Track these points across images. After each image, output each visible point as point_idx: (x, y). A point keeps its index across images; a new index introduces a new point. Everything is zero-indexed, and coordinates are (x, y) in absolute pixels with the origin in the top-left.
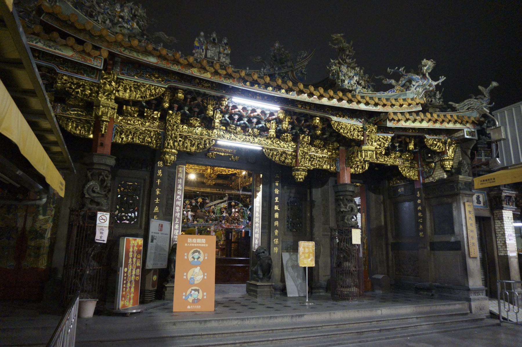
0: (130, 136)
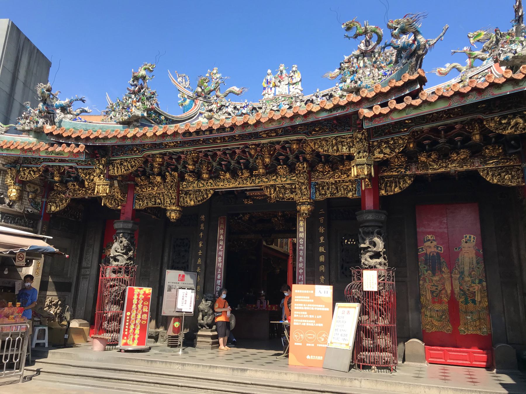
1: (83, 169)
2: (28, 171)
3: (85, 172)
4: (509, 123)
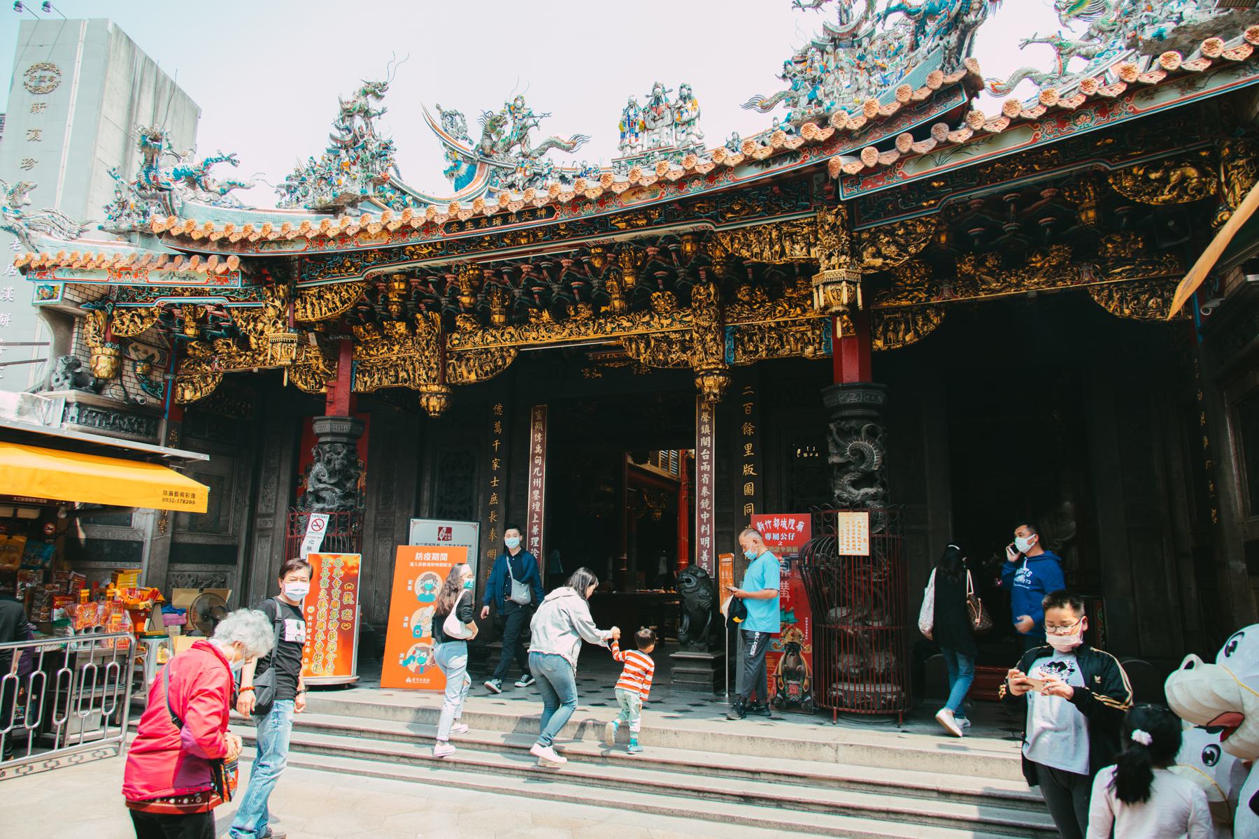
1: (241, 310)
2: (128, 316)
4: (1164, 180)
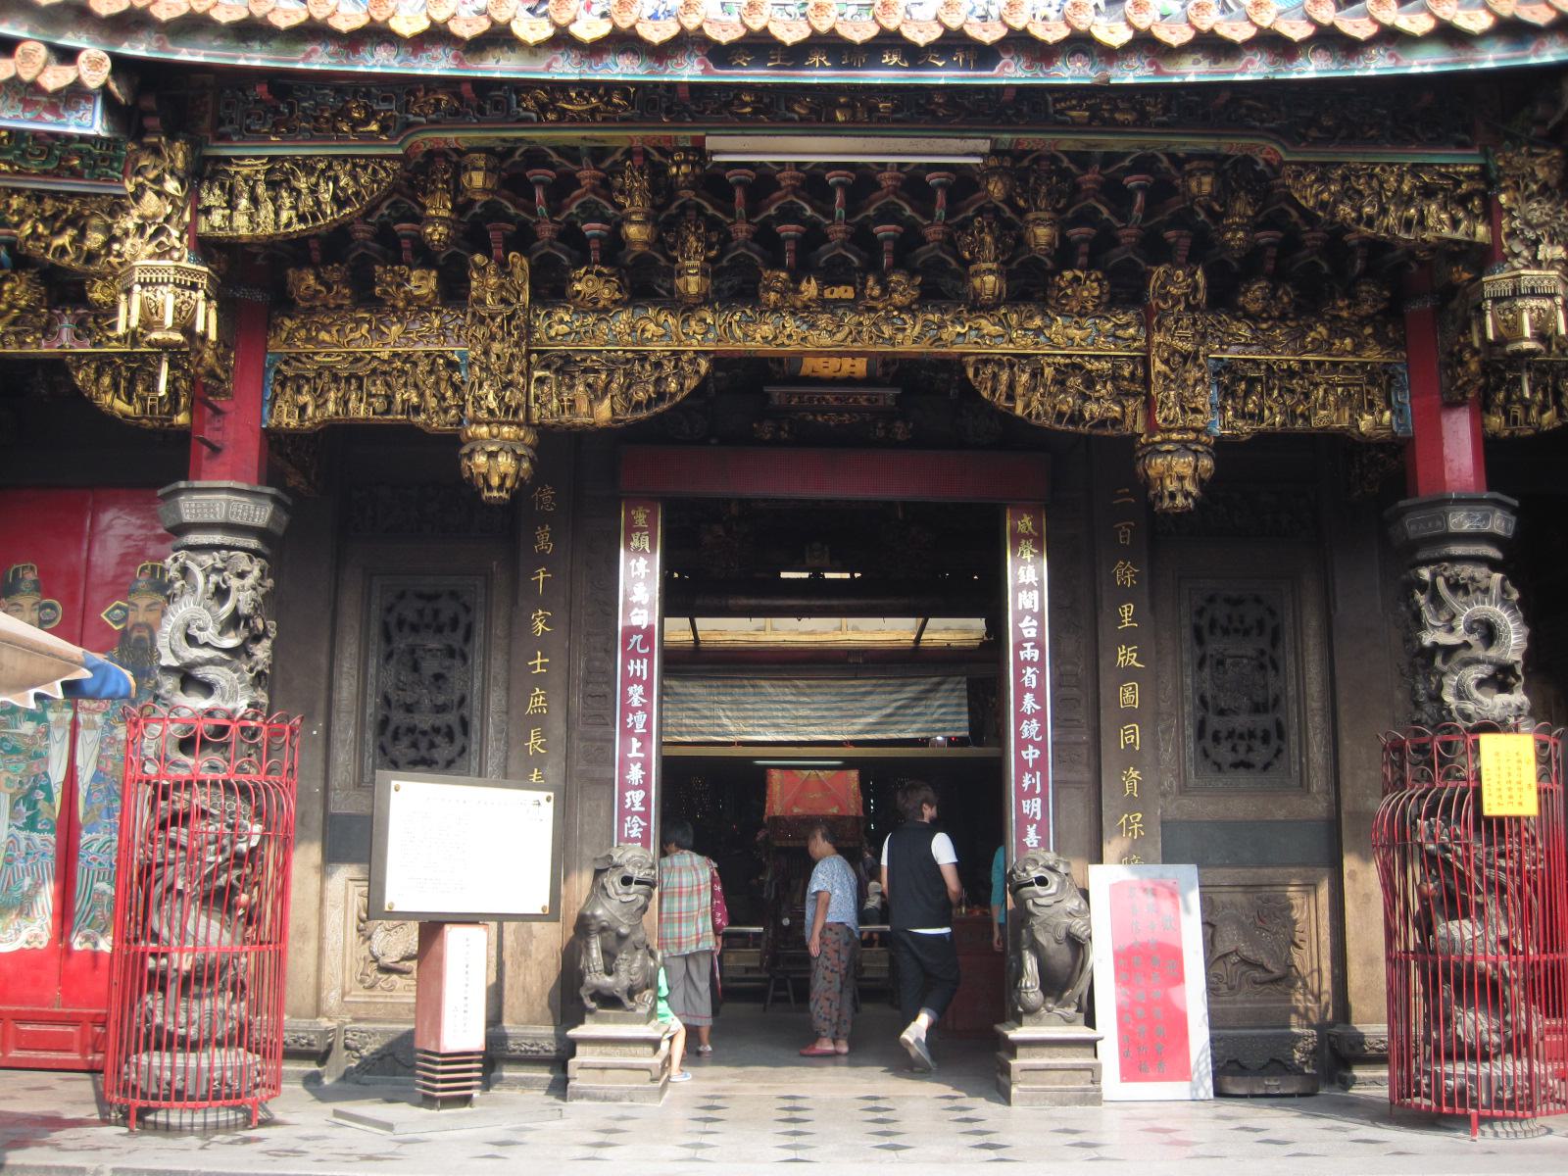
0: (332, 395)
3: (49, 206)
